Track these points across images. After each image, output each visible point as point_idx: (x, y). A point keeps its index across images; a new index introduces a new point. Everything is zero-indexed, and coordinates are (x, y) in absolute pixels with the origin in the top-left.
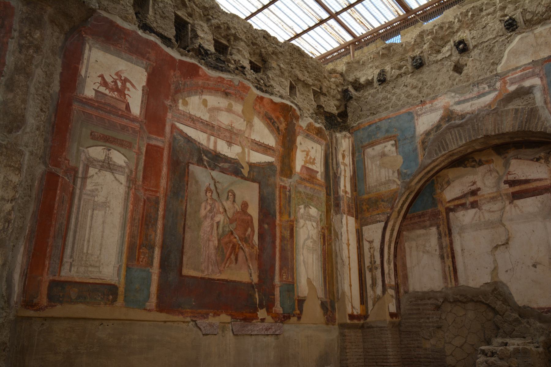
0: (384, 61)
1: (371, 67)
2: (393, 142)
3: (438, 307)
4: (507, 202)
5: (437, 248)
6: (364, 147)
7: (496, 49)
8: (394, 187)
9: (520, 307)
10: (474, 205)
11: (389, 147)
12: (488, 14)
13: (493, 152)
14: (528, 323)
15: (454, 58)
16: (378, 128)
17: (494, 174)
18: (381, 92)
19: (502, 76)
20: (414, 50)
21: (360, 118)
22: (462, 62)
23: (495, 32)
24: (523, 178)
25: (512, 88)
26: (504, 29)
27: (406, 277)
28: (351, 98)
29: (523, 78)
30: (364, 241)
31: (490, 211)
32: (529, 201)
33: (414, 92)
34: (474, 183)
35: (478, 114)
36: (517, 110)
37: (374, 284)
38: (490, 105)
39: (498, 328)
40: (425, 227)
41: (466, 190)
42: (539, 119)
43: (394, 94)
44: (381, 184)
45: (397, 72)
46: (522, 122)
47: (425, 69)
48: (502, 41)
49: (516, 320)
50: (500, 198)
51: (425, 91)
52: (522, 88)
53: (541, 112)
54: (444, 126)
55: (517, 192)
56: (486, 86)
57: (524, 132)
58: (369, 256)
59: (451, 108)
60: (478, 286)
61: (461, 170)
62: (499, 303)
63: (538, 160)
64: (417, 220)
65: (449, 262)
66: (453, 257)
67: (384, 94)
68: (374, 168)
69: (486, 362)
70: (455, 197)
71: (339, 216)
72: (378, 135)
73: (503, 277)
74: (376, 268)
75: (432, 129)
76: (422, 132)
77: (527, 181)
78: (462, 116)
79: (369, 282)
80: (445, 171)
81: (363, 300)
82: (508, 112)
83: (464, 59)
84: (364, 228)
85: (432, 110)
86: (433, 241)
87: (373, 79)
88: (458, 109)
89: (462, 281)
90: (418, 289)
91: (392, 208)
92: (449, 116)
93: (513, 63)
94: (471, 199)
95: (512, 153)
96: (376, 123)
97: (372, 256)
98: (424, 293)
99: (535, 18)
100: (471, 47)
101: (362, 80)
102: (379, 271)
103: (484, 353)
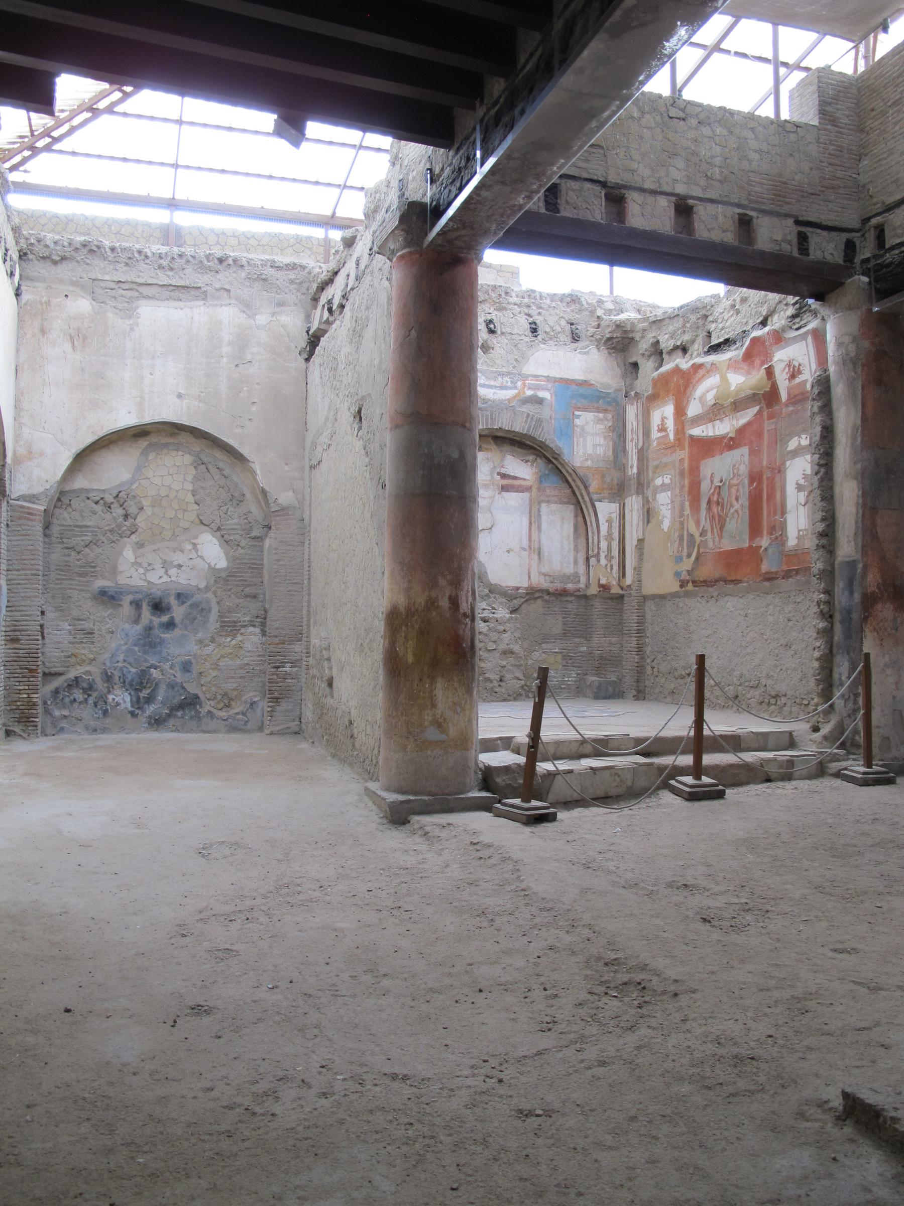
4: (497, 492)
9: (492, 584)
12: (515, 304)
13: (492, 442)
14: (495, 597)
19: (525, 377)
22: (490, 343)
24: (513, 474)
25: (529, 393)
26: (529, 330)
29: (538, 388)
32: (514, 495)
35: (497, 405)
36: (528, 415)
38: (509, 400)
42: (542, 430)
46: (530, 427)
48: (527, 342)
49: (487, 595)
50: (492, 487)
52: (537, 396)
55: (507, 485)
56: (509, 380)
63: (527, 461)
69: (488, 626)
77: (515, 478)
95: (507, 447)
99: (552, 333)
100: (499, 332)
103: (485, 620)
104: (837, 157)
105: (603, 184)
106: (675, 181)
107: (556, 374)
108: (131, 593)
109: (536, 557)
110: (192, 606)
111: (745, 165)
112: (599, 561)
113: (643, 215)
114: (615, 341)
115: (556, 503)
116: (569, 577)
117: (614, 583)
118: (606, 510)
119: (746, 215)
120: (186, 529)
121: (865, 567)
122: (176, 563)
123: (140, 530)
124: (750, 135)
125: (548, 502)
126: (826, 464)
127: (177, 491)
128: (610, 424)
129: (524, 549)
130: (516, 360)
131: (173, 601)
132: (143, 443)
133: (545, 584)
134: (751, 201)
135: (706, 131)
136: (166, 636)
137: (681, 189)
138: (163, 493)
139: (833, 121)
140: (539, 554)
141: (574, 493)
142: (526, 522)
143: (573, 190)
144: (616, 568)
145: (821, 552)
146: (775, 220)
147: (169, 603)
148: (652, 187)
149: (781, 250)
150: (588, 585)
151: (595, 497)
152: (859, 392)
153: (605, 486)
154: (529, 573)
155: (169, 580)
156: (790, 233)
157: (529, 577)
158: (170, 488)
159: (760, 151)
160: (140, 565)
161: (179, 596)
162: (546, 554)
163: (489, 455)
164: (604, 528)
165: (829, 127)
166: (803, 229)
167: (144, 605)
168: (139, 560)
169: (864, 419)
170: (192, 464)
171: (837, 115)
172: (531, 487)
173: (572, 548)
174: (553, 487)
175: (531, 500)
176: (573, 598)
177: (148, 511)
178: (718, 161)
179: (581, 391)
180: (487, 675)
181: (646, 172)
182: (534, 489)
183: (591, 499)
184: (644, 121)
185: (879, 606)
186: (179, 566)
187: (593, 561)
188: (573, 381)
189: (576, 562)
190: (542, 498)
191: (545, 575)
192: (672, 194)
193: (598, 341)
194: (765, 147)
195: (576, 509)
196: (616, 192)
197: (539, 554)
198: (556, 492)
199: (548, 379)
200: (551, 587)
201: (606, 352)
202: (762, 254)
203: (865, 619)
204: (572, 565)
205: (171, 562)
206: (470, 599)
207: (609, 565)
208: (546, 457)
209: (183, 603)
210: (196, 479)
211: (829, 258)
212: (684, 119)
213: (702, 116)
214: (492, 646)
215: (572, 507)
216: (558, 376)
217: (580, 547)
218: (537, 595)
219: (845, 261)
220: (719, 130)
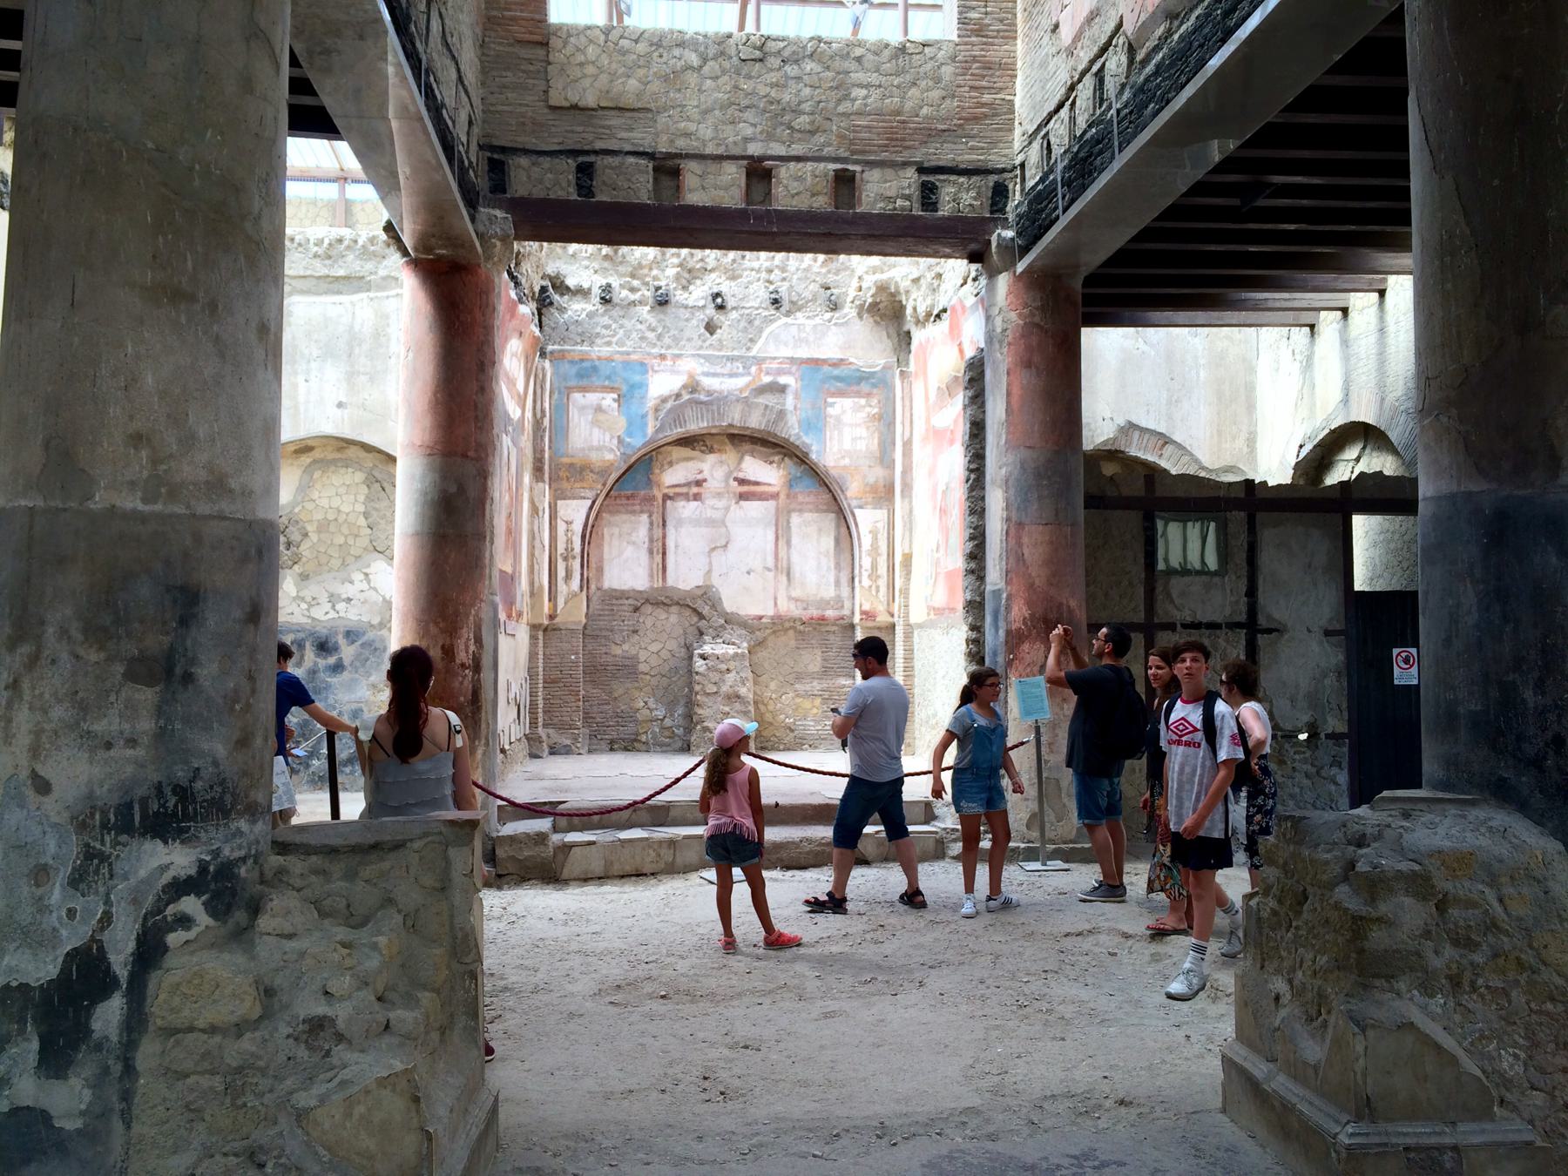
0: (606, 264)
1: (587, 267)
2: (615, 396)
3: (636, 609)
5: (647, 540)
6: (570, 390)
7: (757, 323)
8: (609, 457)
10: (697, 497)
11: (608, 400)
12: (752, 270)
15: (708, 312)
16: (595, 369)
17: (725, 468)
18: (602, 315)
19: (759, 361)
20: (651, 269)
21: (563, 340)
23: (759, 300)
25: (767, 379)
26: (768, 302)
27: (600, 570)
28: (551, 303)
29: (780, 372)
30: (559, 521)
31: (713, 508)
33: (651, 335)
34: (701, 472)
36: (767, 406)
37: (568, 577)
39: (701, 634)
40: (633, 512)
41: (691, 478)
43: (621, 326)
44: (591, 448)
45: (632, 297)
47: (670, 309)
49: (721, 626)
51: (667, 340)
53: (789, 416)
54: (686, 397)
57: (769, 432)
58: (565, 539)
59: (698, 378)
60: (688, 588)
61: (685, 452)
62: (707, 608)
63: (771, 463)
64: (624, 501)
65: (659, 558)
66: (664, 554)
67: (606, 320)
68: (583, 424)
70: (675, 483)
71: (541, 484)
72: (594, 379)
73: (716, 581)
74: (574, 558)
75: (670, 397)
76: (656, 395)
77: (757, 483)
78: (709, 393)
79: (561, 573)
80: (669, 448)
81: (553, 597)
82: (757, 405)
83: (719, 317)
84: (559, 502)
85: (674, 372)
86: (642, 533)
87: (590, 289)
88: (707, 382)
89: (670, 582)
90: (616, 585)
91: (604, 485)
92: (693, 387)
93: (772, 351)
94: (695, 490)
96: (592, 360)
97: (569, 541)
98: (623, 592)
101: (571, 282)
102: (578, 560)
103: (703, 657)
104: (984, 76)
105: (650, 156)
106: (746, 140)
107: (804, 353)
108: (291, 631)
109: (784, 578)
110: (363, 645)
111: (845, 107)
112: (860, 582)
113: (703, 188)
114: (881, 306)
115: (811, 511)
116: (828, 603)
117: (881, 608)
118: (867, 520)
119: (847, 170)
120: (358, 558)
121: (1009, 598)
122: (344, 596)
123: (304, 559)
124: (853, 66)
125: (800, 511)
126: (977, 469)
127: (347, 514)
128: (876, 410)
129: (769, 570)
130: (751, 340)
131: (341, 641)
132: (306, 459)
133: (795, 611)
134: (853, 152)
135: (791, 70)
136: (334, 680)
137: (754, 149)
138: (331, 517)
139: (980, 30)
140: (788, 574)
141: (835, 499)
142: (771, 536)
143: (612, 168)
144: (883, 590)
145: (972, 578)
146: (889, 172)
147: (336, 642)
148: (721, 150)
149: (895, 209)
150: (853, 613)
151: (854, 503)
152: (1005, 378)
153: (868, 489)
154: (776, 599)
155: (336, 616)
156: (909, 185)
157: (776, 604)
158: (339, 511)
159: (867, 86)
160: (303, 599)
161: (348, 634)
162: (797, 575)
163: (724, 457)
164: (866, 541)
165: (974, 39)
166: (931, 178)
167: (308, 645)
168: (301, 594)
169: (1009, 411)
170: (364, 483)
171: (986, 21)
172: (778, 494)
173: (833, 566)
174: (807, 493)
175: (777, 509)
176: (835, 628)
177: (314, 537)
178: (806, 107)
179: (836, 372)
180: (705, 724)
181: (706, 131)
182: (782, 496)
183: (849, 505)
184: (706, 69)
185: (1026, 646)
186: (349, 600)
187: (857, 580)
188: (824, 361)
189: (837, 583)
190: (792, 506)
191: (797, 600)
192: (743, 158)
193: (861, 307)
194: (874, 78)
195: (839, 518)
196: (670, 163)
197: (788, 574)
198: (811, 499)
199: (792, 360)
200: (805, 615)
201: (871, 320)
202: (867, 218)
203: (1009, 664)
204: (832, 589)
205: (339, 596)
206: (472, 648)
207: (874, 588)
208: (797, 457)
209: (353, 642)
210: (369, 499)
211: (967, 213)
212: (761, 60)
213: (786, 54)
214: (712, 689)
215: (833, 515)
216: (805, 355)
217: (843, 564)
218: (787, 625)
219: (992, 213)
220: (809, 66)
